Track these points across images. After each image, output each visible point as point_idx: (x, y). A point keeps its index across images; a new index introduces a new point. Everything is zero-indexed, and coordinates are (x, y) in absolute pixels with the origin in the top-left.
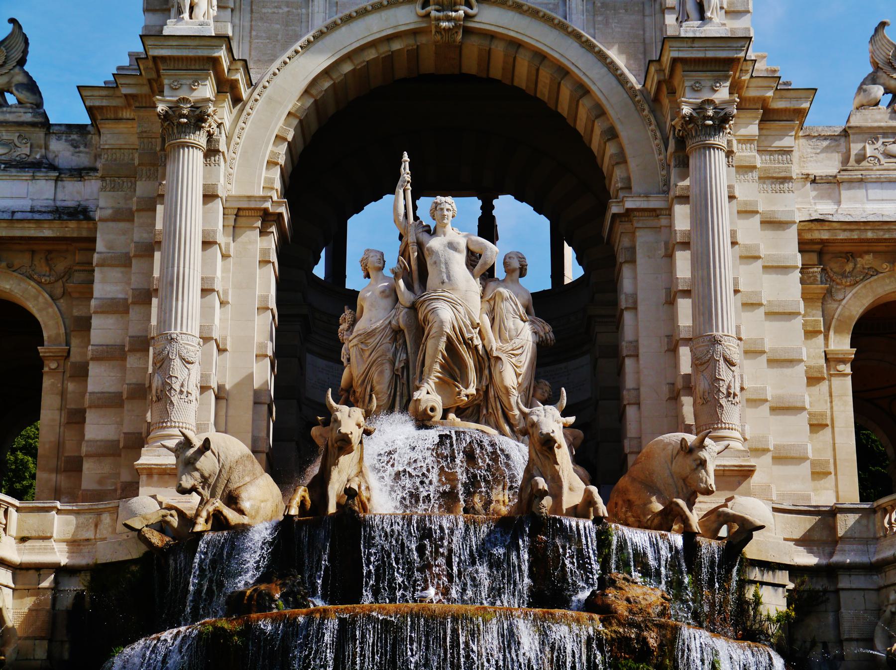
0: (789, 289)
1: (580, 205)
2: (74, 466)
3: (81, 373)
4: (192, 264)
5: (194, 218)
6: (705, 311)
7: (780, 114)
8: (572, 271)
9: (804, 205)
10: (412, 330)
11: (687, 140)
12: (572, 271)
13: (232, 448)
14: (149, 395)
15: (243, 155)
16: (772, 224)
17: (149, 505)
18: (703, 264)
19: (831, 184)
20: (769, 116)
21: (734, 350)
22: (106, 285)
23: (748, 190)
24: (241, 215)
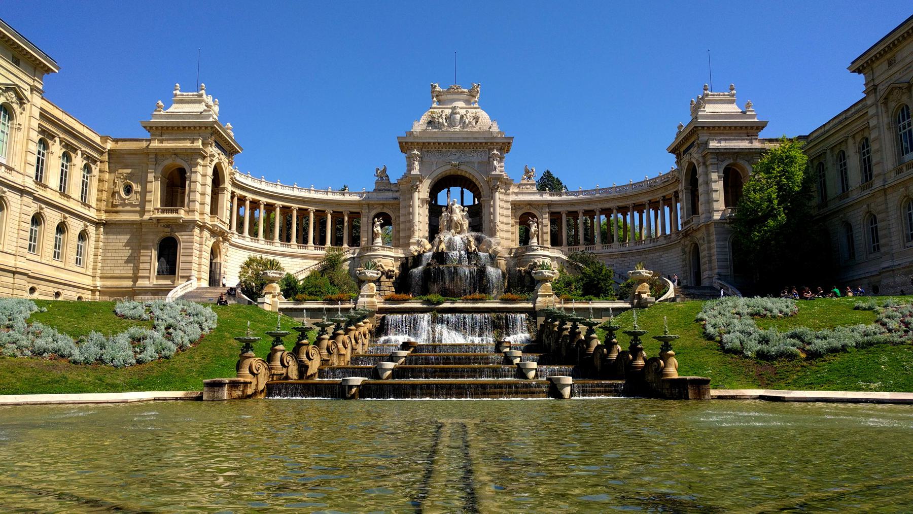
0: (509, 212)
1: (477, 194)
2: (399, 239)
3: (399, 224)
4: (417, 210)
5: (417, 202)
6: (494, 217)
7: (507, 184)
8: (477, 202)
9: (513, 198)
10: (450, 220)
11: (494, 189)
12: (477, 202)
13: (426, 242)
14: (410, 231)
15: (423, 191)
16: (507, 202)
17: (414, 249)
18: (494, 210)
19: (517, 194)
20: (506, 183)
21: (498, 224)
22: (402, 211)
23: (502, 197)
24: (423, 201)
